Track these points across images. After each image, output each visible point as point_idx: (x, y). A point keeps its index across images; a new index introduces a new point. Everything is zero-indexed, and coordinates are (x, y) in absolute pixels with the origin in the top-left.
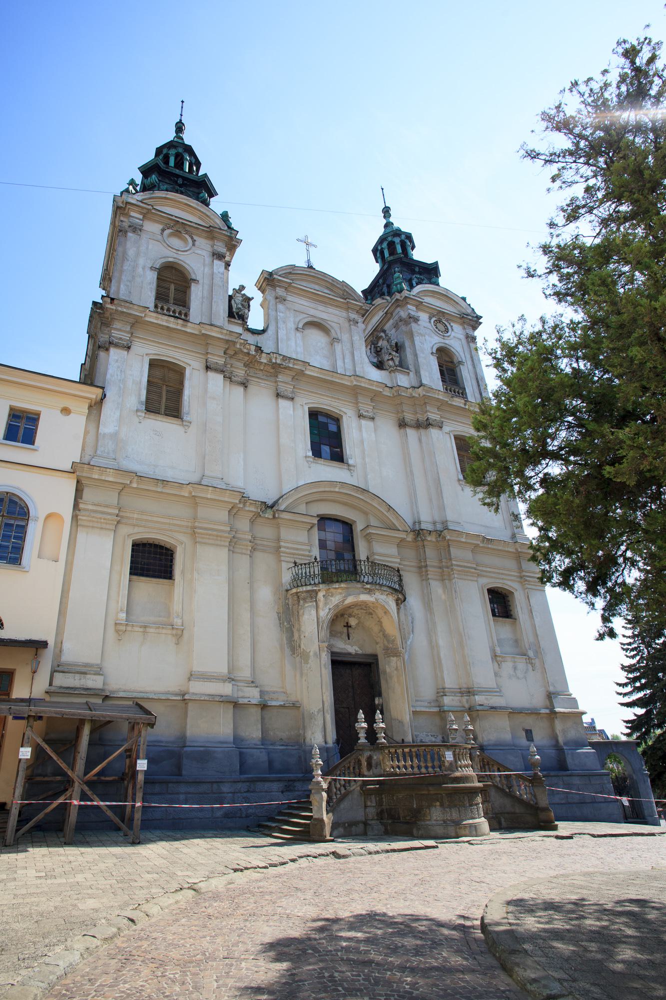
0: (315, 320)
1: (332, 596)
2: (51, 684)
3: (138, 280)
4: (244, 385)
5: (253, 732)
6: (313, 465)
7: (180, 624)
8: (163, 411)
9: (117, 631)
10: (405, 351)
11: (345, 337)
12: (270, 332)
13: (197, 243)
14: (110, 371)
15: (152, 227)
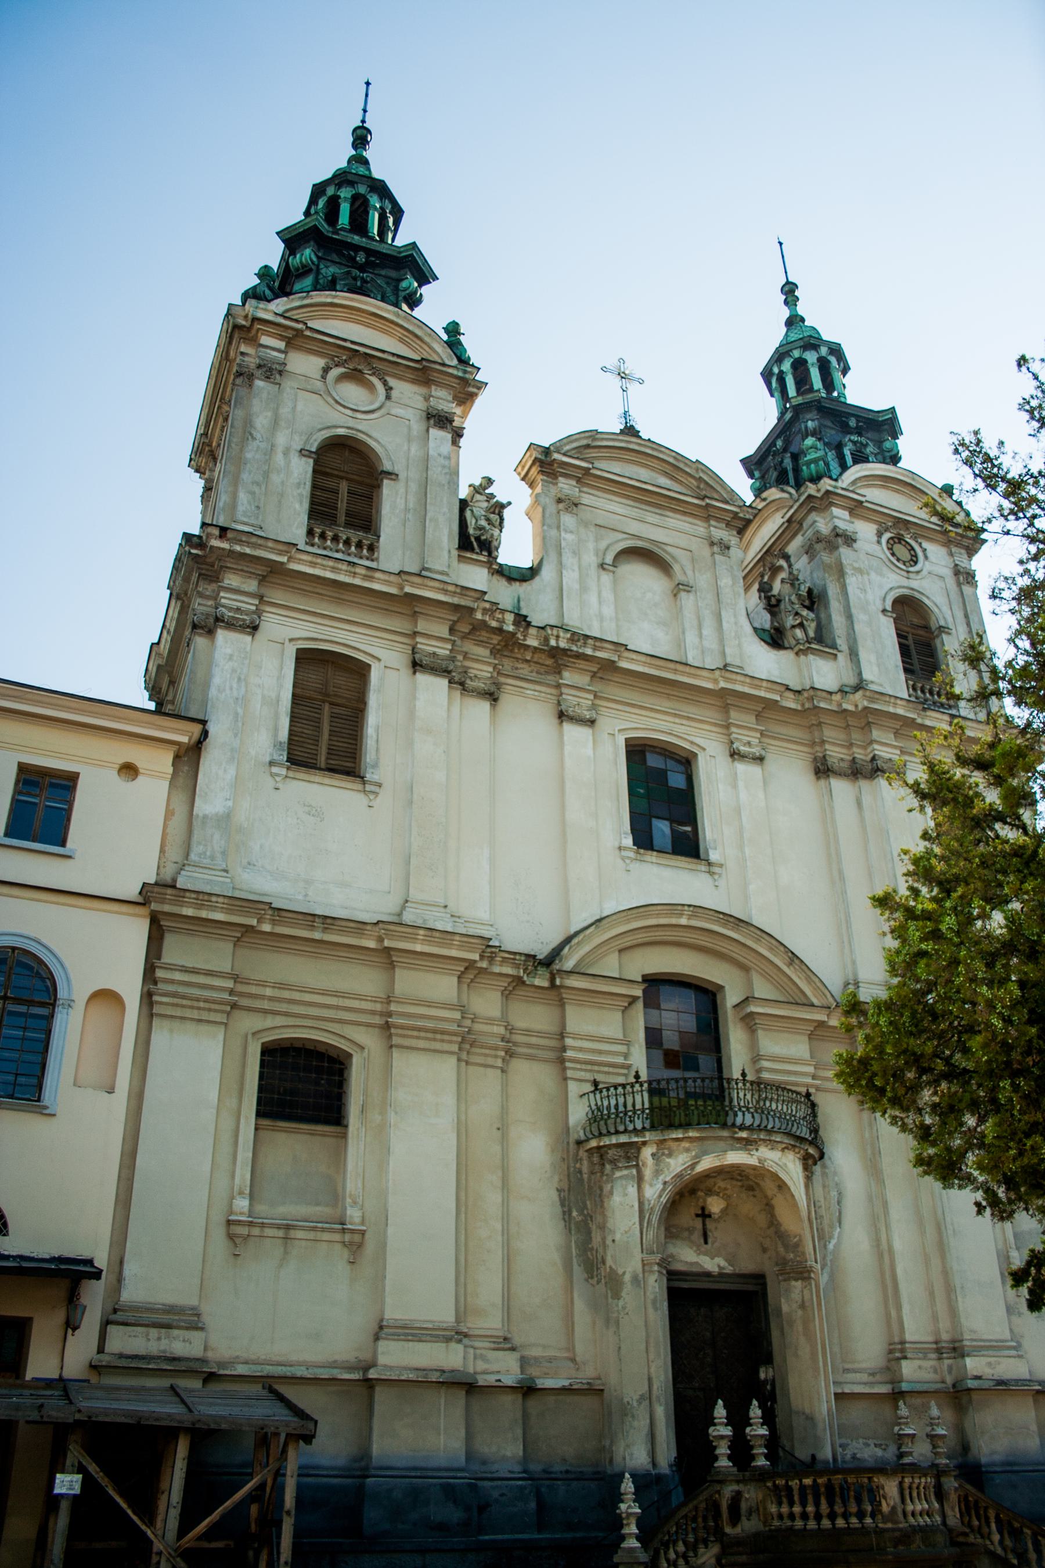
0: (640, 544)
1: (670, 1155)
2: (101, 1350)
3: (276, 478)
4: (492, 696)
5: (504, 1449)
6: (635, 866)
7: (357, 1220)
8: (322, 761)
9: (231, 1237)
10: (827, 606)
11: (702, 580)
12: (547, 573)
13: (394, 394)
14: (216, 681)
15: (305, 365)
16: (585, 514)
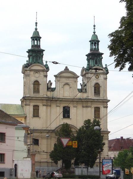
4: (50, 106)
15: (32, 73)
16: (61, 81)
